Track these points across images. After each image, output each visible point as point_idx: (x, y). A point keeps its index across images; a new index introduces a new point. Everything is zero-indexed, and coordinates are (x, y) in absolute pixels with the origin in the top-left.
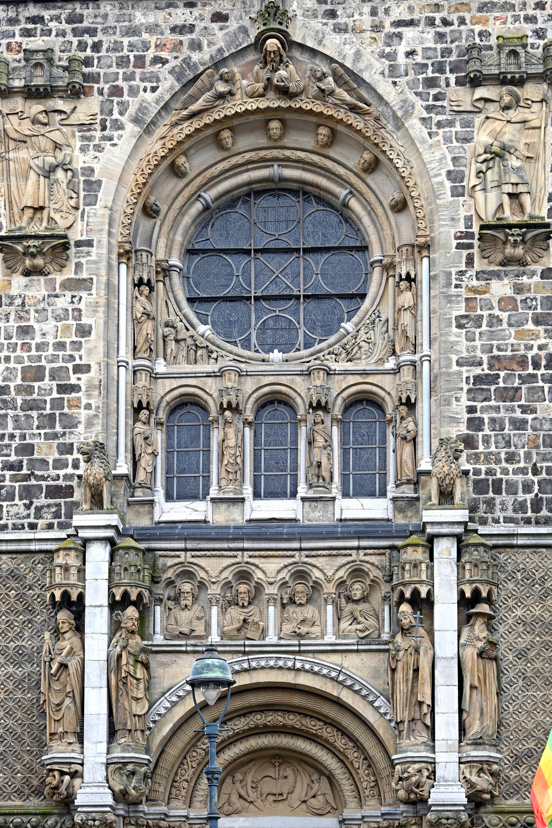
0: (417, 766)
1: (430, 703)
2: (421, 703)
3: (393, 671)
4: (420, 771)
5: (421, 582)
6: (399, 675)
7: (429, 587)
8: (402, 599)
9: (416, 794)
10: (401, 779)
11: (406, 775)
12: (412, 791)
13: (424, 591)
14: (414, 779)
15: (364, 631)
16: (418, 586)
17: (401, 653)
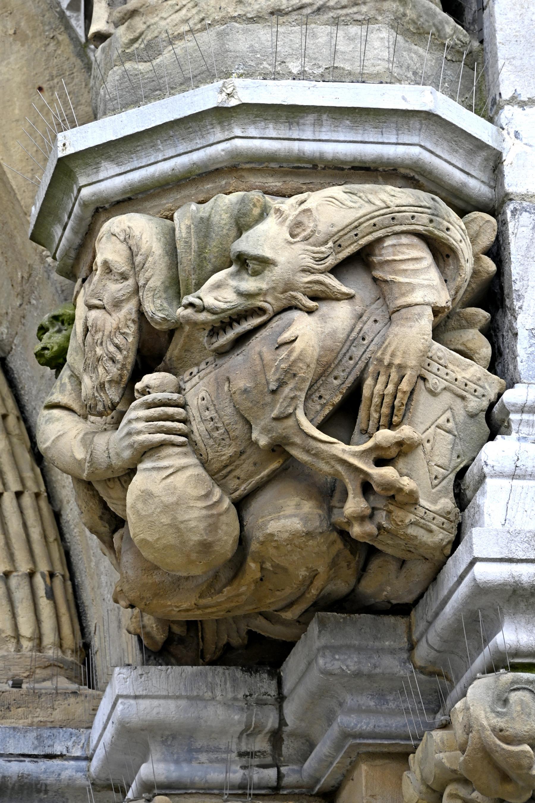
0: (334, 207)
4: (360, 259)
9: (328, 493)
10: (153, 349)
11: (220, 292)
12: (284, 464)
14: (307, 333)
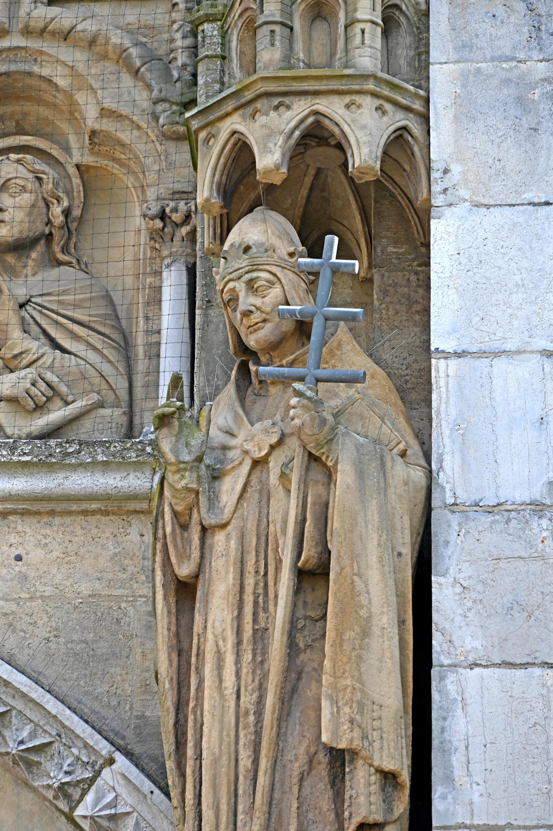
1: (400, 762)
2: (339, 760)
3: (185, 592)
5: (350, 85)
6: (216, 614)
7: (401, 119)
8: (241, 190)
13: (365, 134)
15: (39, 408)
16: (334, 108)
17: (229, 489)
